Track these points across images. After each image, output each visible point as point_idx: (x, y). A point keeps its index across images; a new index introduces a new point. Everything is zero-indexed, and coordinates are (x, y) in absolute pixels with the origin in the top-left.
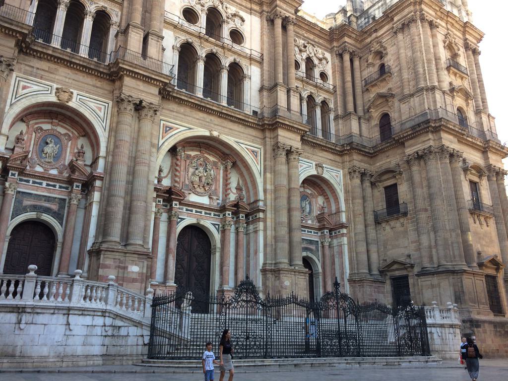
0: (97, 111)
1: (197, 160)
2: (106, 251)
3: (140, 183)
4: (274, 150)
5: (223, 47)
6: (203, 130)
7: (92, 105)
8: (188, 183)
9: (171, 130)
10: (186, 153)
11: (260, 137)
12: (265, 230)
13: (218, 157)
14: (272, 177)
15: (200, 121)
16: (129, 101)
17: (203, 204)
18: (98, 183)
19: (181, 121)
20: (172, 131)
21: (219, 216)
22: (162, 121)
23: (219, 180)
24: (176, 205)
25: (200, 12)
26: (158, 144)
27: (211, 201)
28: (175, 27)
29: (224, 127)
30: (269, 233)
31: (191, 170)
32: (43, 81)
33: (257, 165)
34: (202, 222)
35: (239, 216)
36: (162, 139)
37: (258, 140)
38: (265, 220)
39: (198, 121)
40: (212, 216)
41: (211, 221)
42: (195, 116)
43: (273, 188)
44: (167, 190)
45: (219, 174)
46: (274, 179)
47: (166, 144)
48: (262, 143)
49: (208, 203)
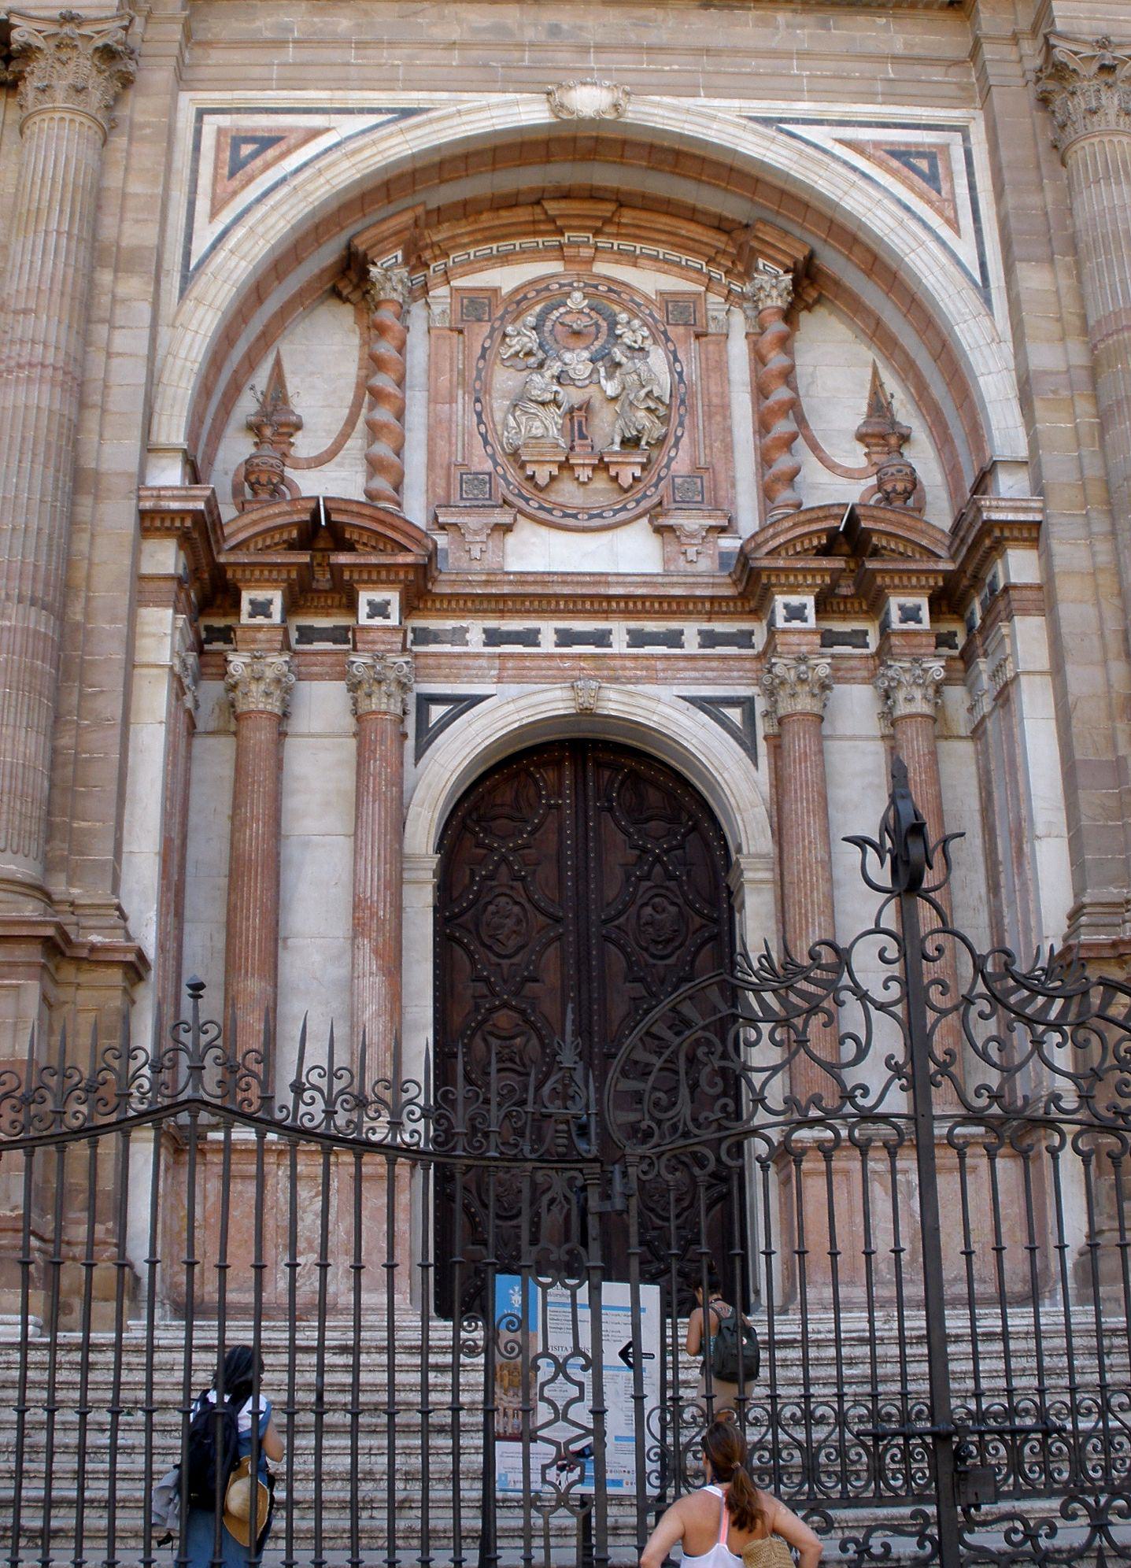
1: (542, 318)
4: (1044, 101)
6: (495, 98)
8: (488, 466)
9: (271, 153)
10: (453, 283)
11: (949, 53)
12: (1057, 669)
14: (1065, 282)
15: (474, 54)
17: (601, 578)
19: (343, 84)
20: (283, 156)
21: (743, 639)
22: (207, 118)
23: (725, 408)
24: (379, 610)
26: (187, 254)
27: (673, 548)
29: (650, 49)
30: (1083, 679)
31: (505, 380)
33: (946, 232)
34: (615, 702)
35: (887, 613)
36: (214, 214)
37: (937, 74)
38: (1044, 598)
39: (455, 57)
40: (692, 645)
41: (685, 681)
42: (438, 33)
43: (1078, 355)
44: (300, 525)
45: (719, 367)
46: (1081, 298)
47: (239, 232)
48: (962, 87)
49: (654, 566)
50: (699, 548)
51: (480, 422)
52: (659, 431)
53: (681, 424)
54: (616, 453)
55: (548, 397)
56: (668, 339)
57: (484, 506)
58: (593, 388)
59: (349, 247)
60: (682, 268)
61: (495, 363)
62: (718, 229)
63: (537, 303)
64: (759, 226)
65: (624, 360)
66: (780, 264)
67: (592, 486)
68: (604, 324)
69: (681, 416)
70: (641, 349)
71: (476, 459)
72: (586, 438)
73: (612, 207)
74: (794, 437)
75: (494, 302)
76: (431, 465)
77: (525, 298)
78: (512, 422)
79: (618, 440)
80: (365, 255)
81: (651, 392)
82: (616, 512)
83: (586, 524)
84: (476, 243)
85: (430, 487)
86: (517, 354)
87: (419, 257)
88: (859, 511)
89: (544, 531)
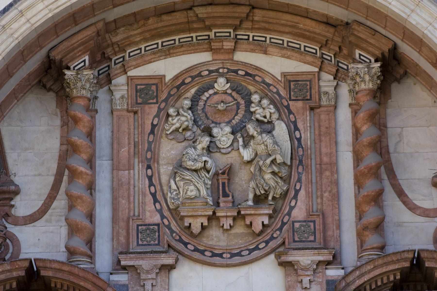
1: (195, 100)
8: (157, 219)
13: (314, 47)
27: (293, 278)
50: (312, 278)
51: (151, 184)
52: (282, 187)
53: (299, 180)
54: (250, 207)
55: (199, 165)
56: (290, 112)
57: (152, 252)
58: (234, 154)
59: (48, 56)
60: (301, 53)
61: (161, 137)
62: (327, 24)
63: (193, 87)
64: (355, 26)
65: (255, 134)
66: (373, 55)
67: (233, 231)
68: (242, 102)
69: (299, 173)
70: (270, 122)
71: (148, 214)
72: (228, 196)
73: (246, 10)
74: (380, 193)
75: (160, 86)
76: (115, 219)
77: (183, 83)
78: (174, 186)
79: (251, 196)
80: (61, 61)
81: (275, 159)
82: (251, 251)
83: (230, 262)
84: (146, 40)
85: (114, 236)
86: (177, 130)
87: (104, 53)
88: (423, 255)
89: (198, 267)
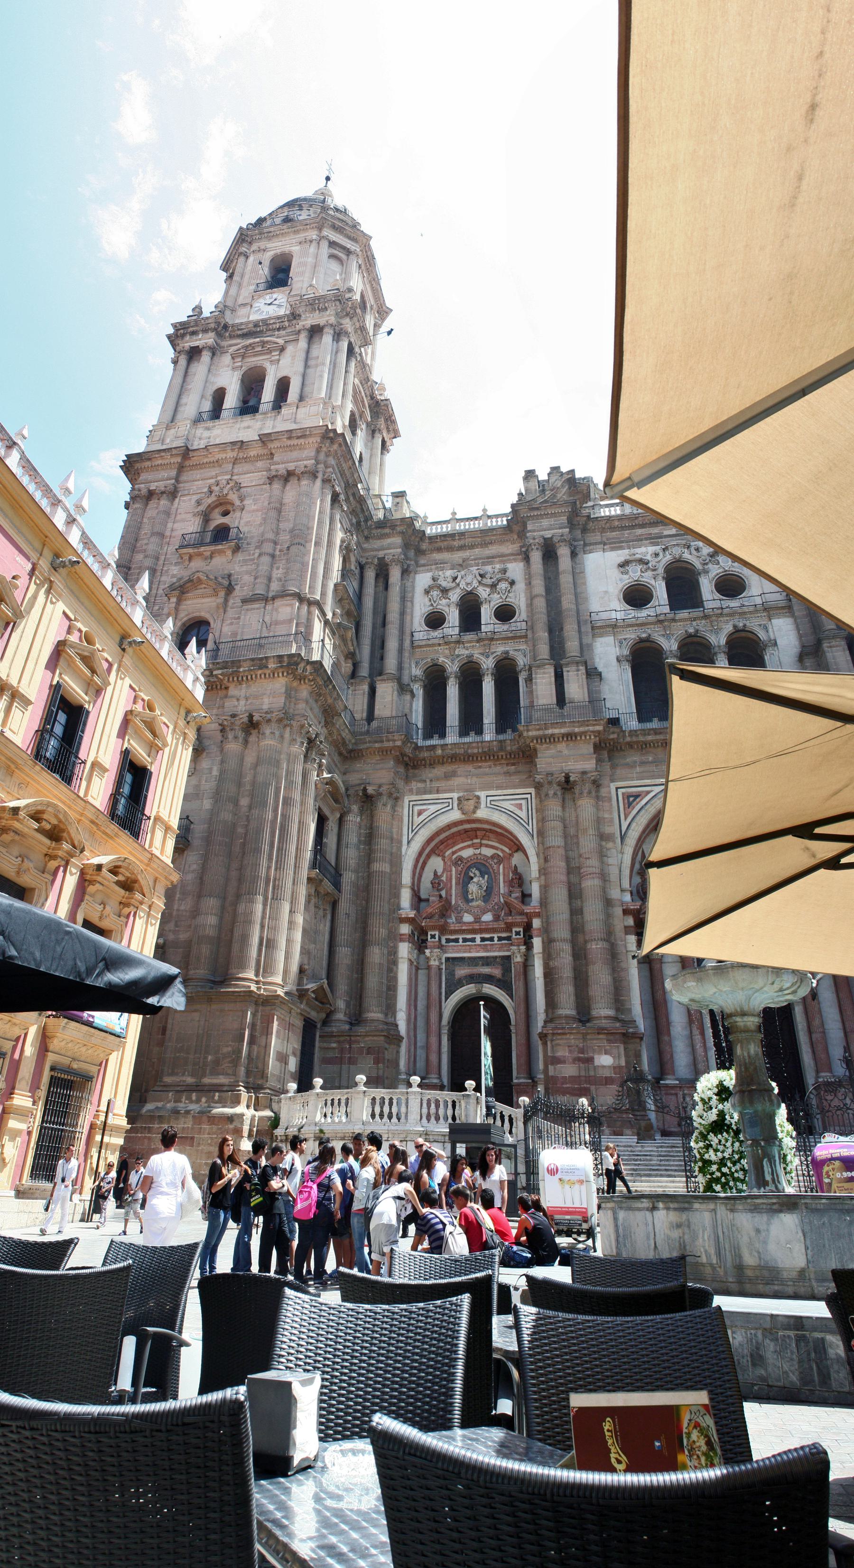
0: (518, 812)
2: (553, 1034)
3: (593, 912)
5: (706, 617)
7: (507, 805)
16: (550, 783)
18: (536, 923)
25: (652, 582)
28: (613, 627)
32: (441, 796)
36: (626, 819)
47: (634, 825)
